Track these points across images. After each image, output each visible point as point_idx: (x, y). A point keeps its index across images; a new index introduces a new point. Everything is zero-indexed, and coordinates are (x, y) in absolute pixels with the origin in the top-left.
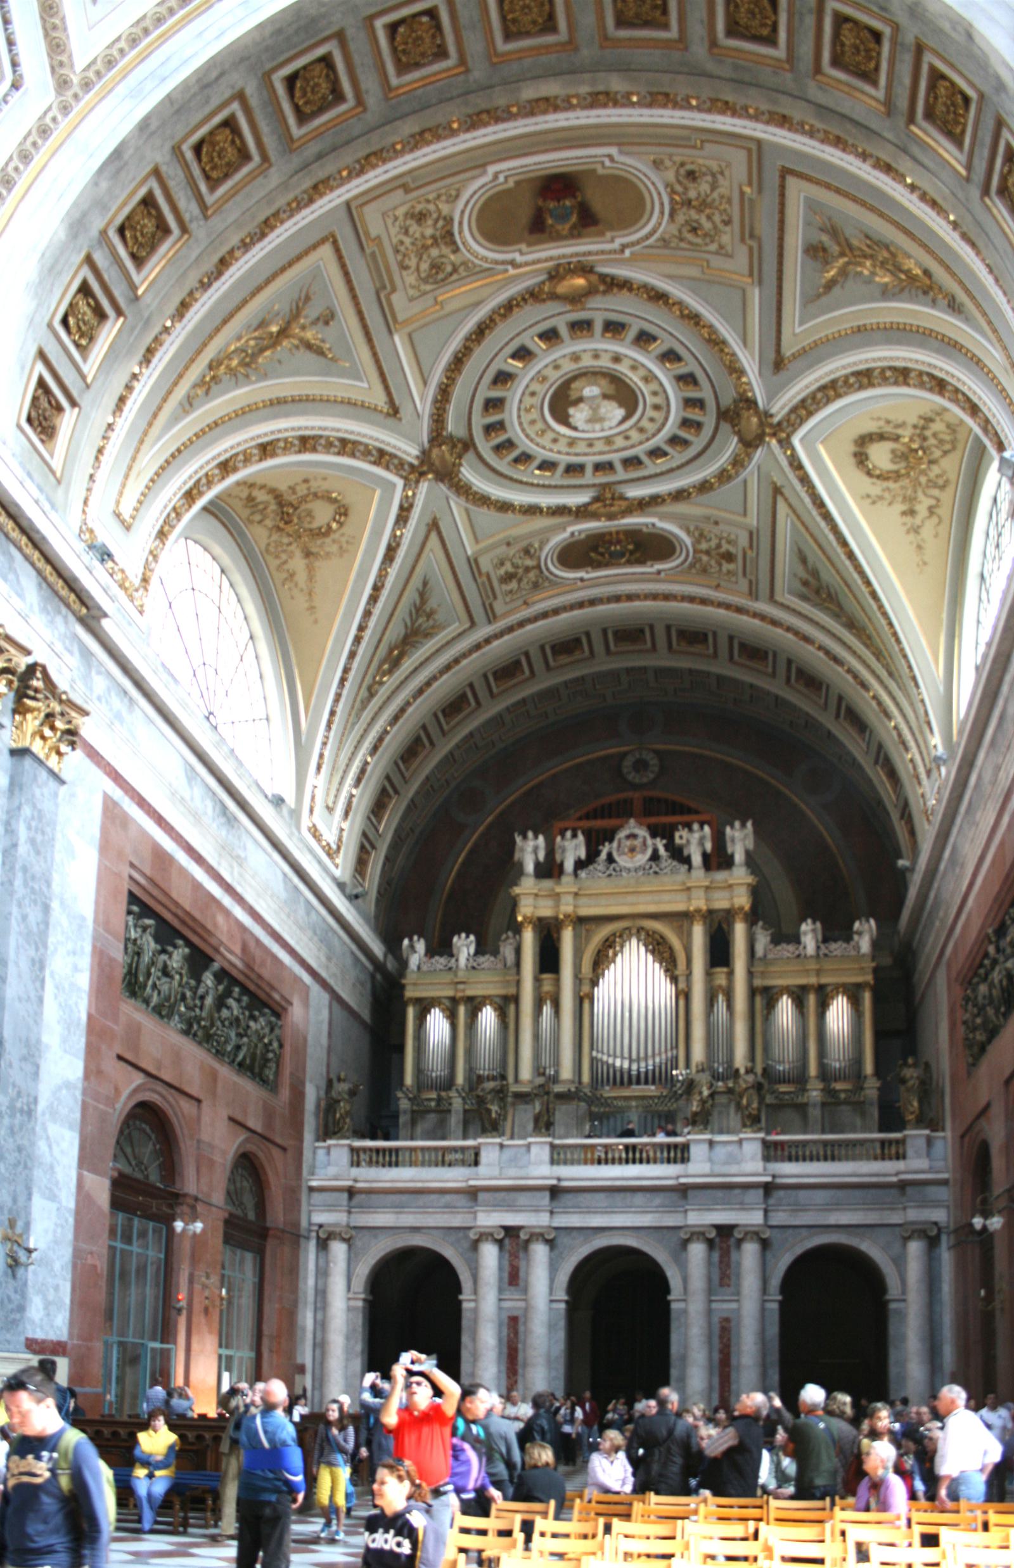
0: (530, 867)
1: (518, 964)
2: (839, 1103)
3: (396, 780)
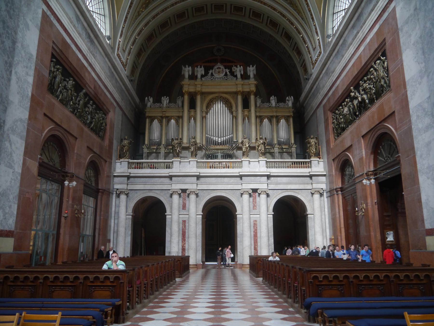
0: (187, 76)
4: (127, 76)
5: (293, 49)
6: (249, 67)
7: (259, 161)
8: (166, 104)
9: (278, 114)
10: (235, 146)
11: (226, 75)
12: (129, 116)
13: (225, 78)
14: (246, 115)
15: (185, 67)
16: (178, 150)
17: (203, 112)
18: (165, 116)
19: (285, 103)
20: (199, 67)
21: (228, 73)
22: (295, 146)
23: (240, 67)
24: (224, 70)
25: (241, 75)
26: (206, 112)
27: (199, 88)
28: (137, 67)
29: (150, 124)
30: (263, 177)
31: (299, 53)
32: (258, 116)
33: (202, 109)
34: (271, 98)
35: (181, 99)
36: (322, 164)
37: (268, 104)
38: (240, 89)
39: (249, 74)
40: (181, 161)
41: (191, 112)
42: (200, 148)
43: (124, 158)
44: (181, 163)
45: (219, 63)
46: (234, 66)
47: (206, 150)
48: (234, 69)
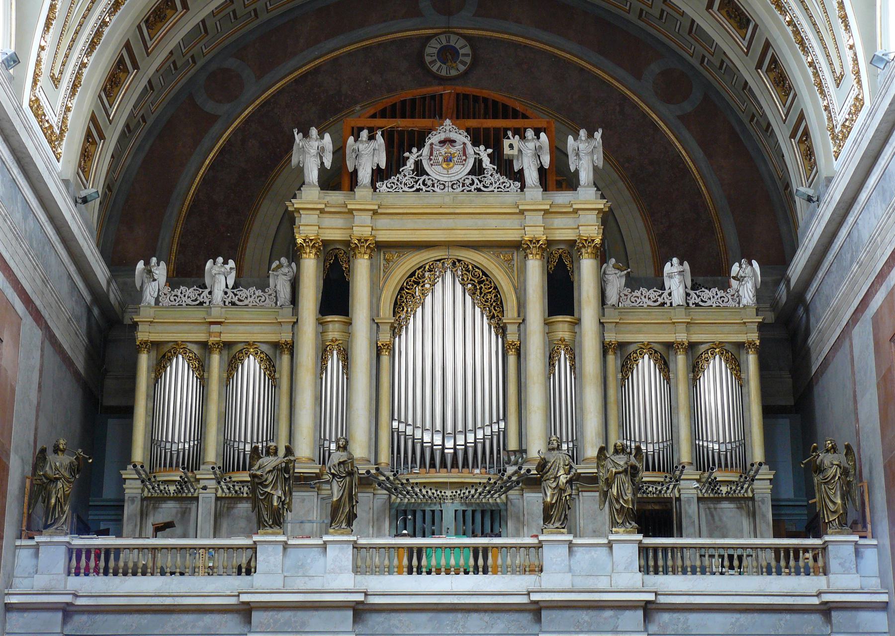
0: (312, 175)
1: (294, 300)
2: (719, 500)
3: (137, 49)
4: (66, 182)
5: (759, 66)
6: (576, 137)
7: (610, 545)
8: (226, 293)
9: (695, 338)
10: (513, 474)
11: (478, 170)
12: (66, 346)
13: (472, 184)
14: (560, 340)
15: (306, 135)
16: (279, 498)
17: (381, 327)
18: (218, 343)
19: (725, 290)
20: (364, 134)
21: (486, 162)
22: (766, 473)
23: (538, 138)
24: (470, 149)
25: (541, 171)
26: (392, 324)
27: (362, 227)
28: (102, 137)
29: (153, 375)
30: (628, 613)
31: (782, 82)
32: (610, 344)
33: (378, 315)
34: (667, 268)
35: (285, 270)
36: (871, 557)
37: (652, 293)
38: (535, 230)
39: (572, 169)
40: (290, 542)
41: (331, 326)
42: (367, 481)
43: (52, 529)
44: (289, 550)
45: (448, 122)
46: (510, 134)
47: (393, 489)
48: (511, 146)
